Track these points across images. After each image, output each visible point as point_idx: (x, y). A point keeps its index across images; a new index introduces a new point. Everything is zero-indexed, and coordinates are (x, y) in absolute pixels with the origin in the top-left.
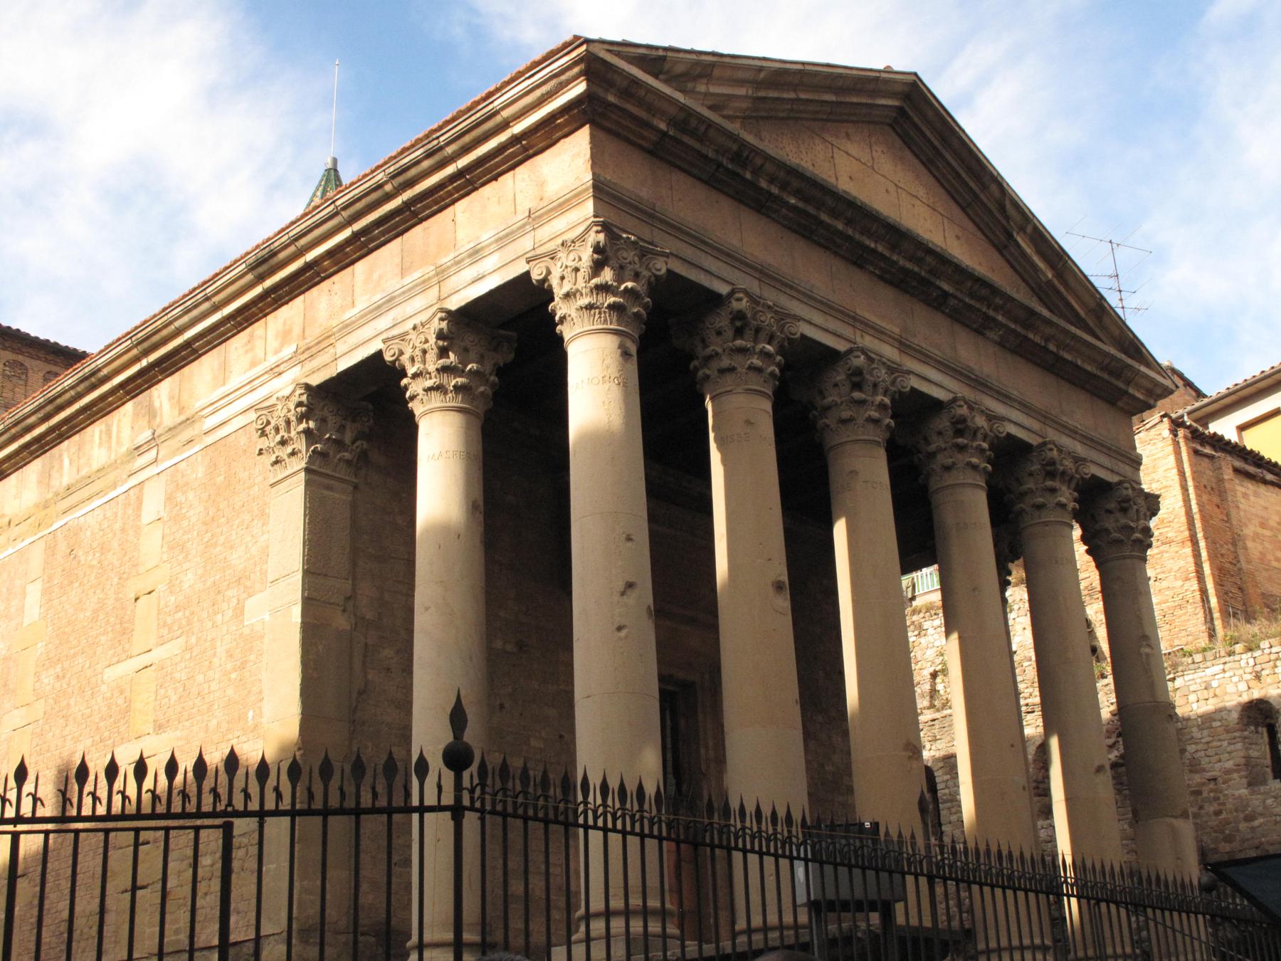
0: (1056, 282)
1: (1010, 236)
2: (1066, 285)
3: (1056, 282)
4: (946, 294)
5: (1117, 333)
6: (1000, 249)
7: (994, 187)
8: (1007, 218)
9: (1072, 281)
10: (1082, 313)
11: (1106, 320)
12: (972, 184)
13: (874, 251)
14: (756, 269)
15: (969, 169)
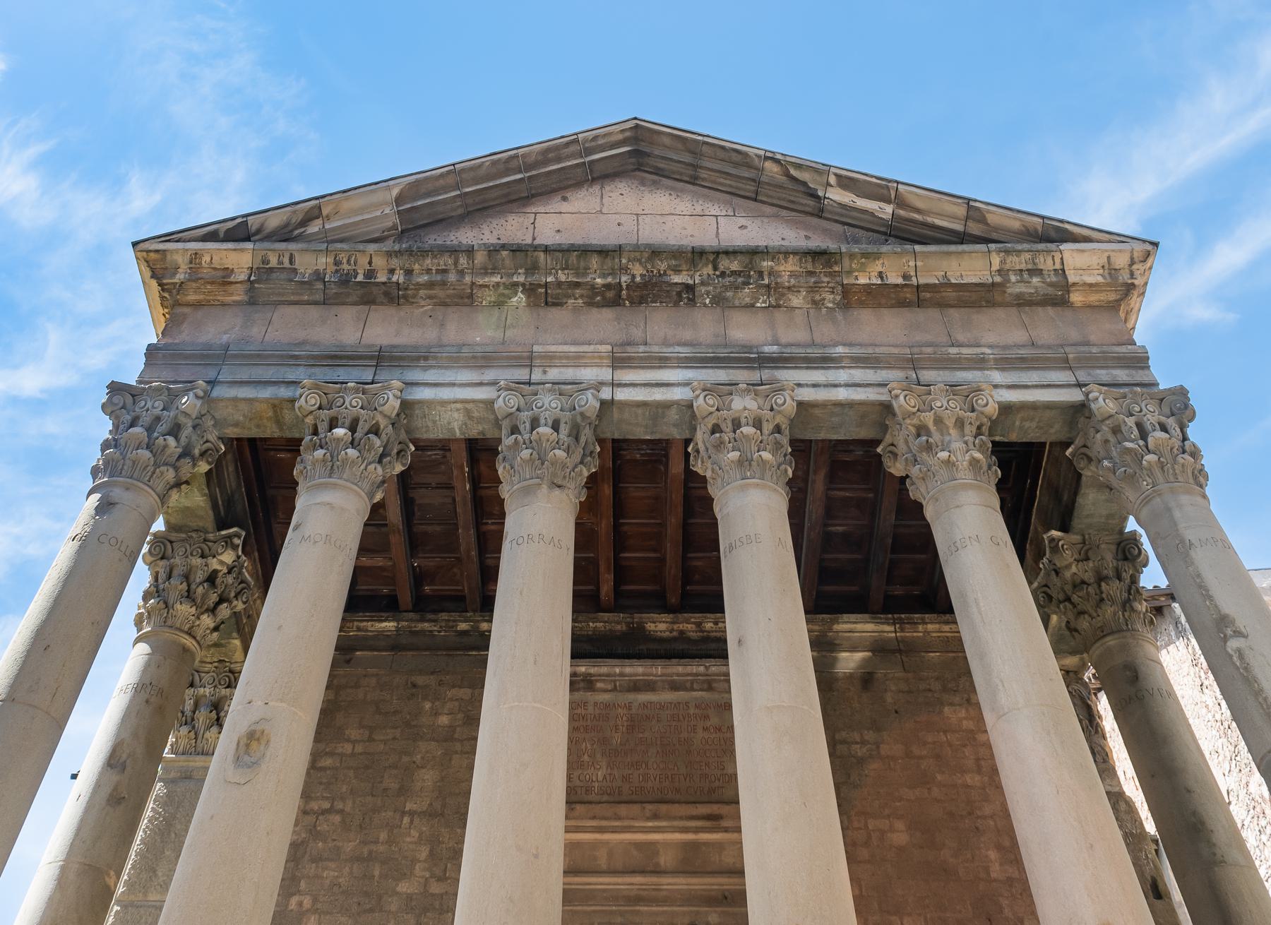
0: (902, 212)
1: (818, 197)
2: (918, 211)
3: (902, 212)
4: (690, 288)
5: (1016, 225)
6: (819, 213)
7: (768, 164)
8: (804, 184)
9: (919, 204)
10: (959, 227)
11: (991, 218)
12: (746, 175)
13: (559, 284)
14: (371, 358)
15: (736, 165)
